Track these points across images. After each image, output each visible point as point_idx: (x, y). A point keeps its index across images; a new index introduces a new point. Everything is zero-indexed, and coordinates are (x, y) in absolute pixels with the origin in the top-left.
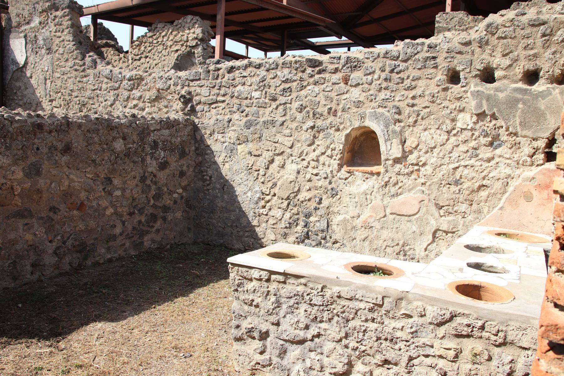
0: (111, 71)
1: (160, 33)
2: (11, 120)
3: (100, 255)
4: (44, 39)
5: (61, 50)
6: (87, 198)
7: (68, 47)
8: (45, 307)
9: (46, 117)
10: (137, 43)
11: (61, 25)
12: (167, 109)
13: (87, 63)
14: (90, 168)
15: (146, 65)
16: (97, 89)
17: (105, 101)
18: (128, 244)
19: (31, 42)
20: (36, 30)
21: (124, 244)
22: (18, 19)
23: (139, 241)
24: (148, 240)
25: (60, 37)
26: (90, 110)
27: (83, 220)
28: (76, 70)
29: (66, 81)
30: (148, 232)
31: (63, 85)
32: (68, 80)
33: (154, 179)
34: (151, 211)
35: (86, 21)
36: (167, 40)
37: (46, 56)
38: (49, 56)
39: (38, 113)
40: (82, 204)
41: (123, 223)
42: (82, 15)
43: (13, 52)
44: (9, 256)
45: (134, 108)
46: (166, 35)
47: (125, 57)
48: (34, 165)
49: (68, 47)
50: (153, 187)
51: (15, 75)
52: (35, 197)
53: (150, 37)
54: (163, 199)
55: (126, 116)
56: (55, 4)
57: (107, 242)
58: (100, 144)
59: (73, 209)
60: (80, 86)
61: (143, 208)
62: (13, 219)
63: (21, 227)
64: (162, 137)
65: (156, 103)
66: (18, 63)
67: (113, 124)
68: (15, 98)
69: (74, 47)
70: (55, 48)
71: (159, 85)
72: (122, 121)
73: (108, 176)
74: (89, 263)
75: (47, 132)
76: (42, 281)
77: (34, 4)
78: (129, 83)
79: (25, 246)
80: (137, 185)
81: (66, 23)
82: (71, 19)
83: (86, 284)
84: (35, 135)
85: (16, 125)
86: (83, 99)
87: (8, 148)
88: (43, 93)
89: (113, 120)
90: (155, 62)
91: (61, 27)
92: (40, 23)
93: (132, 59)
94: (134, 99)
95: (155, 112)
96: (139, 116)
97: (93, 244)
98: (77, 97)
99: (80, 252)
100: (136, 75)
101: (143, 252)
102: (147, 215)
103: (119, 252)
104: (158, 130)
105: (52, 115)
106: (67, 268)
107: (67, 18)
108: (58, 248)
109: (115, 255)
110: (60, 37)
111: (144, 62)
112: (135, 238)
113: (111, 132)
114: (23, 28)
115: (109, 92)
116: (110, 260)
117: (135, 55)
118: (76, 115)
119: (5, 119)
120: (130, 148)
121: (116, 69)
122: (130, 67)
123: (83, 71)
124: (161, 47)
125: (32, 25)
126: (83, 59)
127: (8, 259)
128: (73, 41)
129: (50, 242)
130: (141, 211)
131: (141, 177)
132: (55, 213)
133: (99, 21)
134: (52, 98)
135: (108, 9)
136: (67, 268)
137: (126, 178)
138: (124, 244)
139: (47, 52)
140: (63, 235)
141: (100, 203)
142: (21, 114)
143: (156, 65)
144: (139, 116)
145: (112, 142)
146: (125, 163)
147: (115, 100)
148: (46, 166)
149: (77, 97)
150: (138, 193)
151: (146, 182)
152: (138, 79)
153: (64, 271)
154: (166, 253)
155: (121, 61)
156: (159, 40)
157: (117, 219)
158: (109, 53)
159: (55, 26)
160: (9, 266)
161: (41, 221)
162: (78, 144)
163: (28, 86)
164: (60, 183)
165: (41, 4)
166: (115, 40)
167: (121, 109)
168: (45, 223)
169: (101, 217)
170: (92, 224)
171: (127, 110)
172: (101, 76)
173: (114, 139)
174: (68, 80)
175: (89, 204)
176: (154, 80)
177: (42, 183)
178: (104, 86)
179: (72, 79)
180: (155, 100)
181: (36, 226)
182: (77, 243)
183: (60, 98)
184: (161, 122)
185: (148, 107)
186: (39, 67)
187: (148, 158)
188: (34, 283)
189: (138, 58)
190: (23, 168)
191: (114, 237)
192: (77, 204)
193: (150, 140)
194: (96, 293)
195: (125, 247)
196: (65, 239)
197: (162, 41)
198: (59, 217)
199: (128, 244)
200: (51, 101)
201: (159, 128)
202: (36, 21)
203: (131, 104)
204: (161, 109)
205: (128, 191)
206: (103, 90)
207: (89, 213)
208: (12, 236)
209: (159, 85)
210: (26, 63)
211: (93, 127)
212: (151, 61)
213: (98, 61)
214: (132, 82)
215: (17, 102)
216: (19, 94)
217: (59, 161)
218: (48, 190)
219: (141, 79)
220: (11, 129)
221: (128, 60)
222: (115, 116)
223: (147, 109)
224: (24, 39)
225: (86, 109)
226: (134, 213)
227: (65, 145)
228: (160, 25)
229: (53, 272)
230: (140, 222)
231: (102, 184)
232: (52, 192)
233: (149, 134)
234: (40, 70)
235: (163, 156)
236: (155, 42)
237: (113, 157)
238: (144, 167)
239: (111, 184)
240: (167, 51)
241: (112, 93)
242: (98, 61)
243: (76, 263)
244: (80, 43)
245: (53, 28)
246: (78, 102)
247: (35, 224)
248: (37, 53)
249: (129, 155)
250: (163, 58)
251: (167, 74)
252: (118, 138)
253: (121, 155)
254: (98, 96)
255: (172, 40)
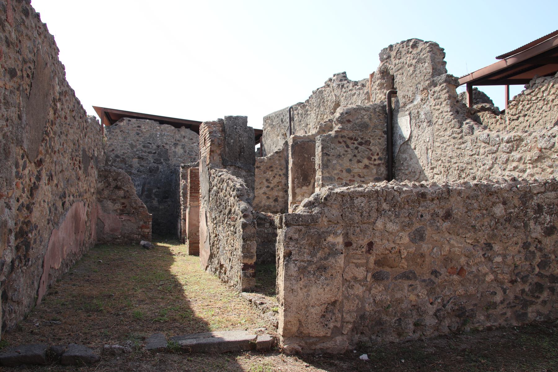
0: (488, 135)
1: (540, 89)
2: (400, 191)
3: (479, 322)
4: (425, 114)
5: (440, 122)
6: (467, 263)
7: (446, 117)
8: (425, 367)
9: (428, 186)
10: (513, 103)
11: (439, 98)
12: (552, 169)
13: (464, 130)
14: (469, 234)
15: (525, 124)
16: (474, 154)
17: (484, 165)
18: (509, 314)
19: (414, 117)
20: (419, 106)
21: (505, 314)
22: (404, 100)
23: (522, 311)
24: (532, 312)
25: (439, 109)
26: (469, 175)
27: (463, 285)
28: (454, 138)
29: (445, 149)
30: (532, 303)
31: (443, 153)
32: (447, 148)
33: (539, 246)
34: (536, 280)
35: (461, 89)
36: (548, 95)
37: (427, 128)
38: (430, 128)
39: (422, 183)
40: (462, 269)
41: (504, 291)
42: (457, 85)
43: (400, 129)
44: (395, 313)
45: (514, 170)
46: (546, 90)
47: (501, 119)
48: (418, 231)
49: (446, 117)
50: (538, 254)
51: (402, 148)
52: (418, 260)
53: (527, 95)
54: (550, 267)
55: (506, 181)
56: (433, 81)
57: (487, 309)
58: (479, 210)
59: (453, 273)
60: (459, 153)
61: (527, 276)
62: (400, 280)
63: (406, 288)
64: (546, 200)
65: (539, 164)
66: (404, 138)
67: (493, 189)
68: (402, 168)
69: (452, 117)
70: (434, 120)
71: (541, 144)
72: (502, 186)
73: (489, 241)
74: (468, 328)
75: (429, 200)
76: (422, 340)
77: (416, 85)
78: (508, 145)
79: (409, 305)
80: (519, 252)
81: (444, 95)
82: (448, 92)
83: (464, 350)
84: (419, 203)
85: (403, 195)
86: (461, 165)
87: (397, 216)
88: (425, 162)
89: (492, 185)
90: (535, 119)
91: (440, 100)
92: (422, 100)
93: (509, 120)
94: (513, 161)
95: (537, 173)
96: (520, 179)
97: (472, 310)
98: (456, 163)
99: (459, 316)
100: (515, 136)
101: (527, 324)
102: (531, 284)
103: (500, 321)
104: (542, 193)
105: (434, 184)
106: (446, 331)
107: (445, 91)
108: (438, 310)
109: (495, 324)
110: (439, 109)
111: (523, 121)
112: (517, 308)
113: (490, 197)
114: (408, 107)
115: (487, 156)
116: (490, 329)
117: (512, 115)
118: (456, 182)
119: (395, 190)
120: (511, 213)
121: (493, 132)
122: (507, 129)
123: (460, 138)
124: (541, 103)
125: (415, 103)
126: (460, 127)
127: (395, 316)
128: (450, 111)
129: (431, 304)
130: (524, 279)
131: (524, 243)
132: (436, 276)
133: (474, 87)
134: (433, 166)
135: (483, 75)
136: (446, 331)
137: (507, 244)
138: (505, 314)
139: (428, 124)
140: (443, 298)
141: (479, 269)
142: (408, 185)
143: (536, 122)
144: (520, 179)
145: (491, 207)
146: (505, 228)
147: (493, 164)
148: (428, 232)
149: (456, 163)
150: (520, 260)
151: (530, 249)
152: (517, 140)
153: (443, 334)
154: (555, 329)
155: (498, 123)
156: (538, 96)
157: (498, 286)
158: (486, 117)
159: (434, 100)
160: (395, 323)
161: (423, 284)
162: (458, 211)
163: (412, 156)
164: (441, 248)
165: (422, 83)
166: (490, 102)
167: (500, 172)
168: (427, 286)
169: (480, 283)
170: (472, 289)
171: (507, 173)
172: (478, 141)
173: (494, 204)
174: (447, 148)
175: (469, 269)
176: (535, 139)
177: (425, 247)
178: (482, 151)
179: (451, 147)
180: (536, 161)
181: (419, 288)
182: (457, 307)
183: (440, 165)
184: (545, 184)
185: (530, 168)
186: (422, 139)
187: (532, 223)
188: (416, 341)
189: (515, 117)
190: (409, 234)
191: (494, 305)
192: (457, 269)
193: (533, 203)
194: (474, 361)
195: (506, 316)
196: (445, 302)
197: (543, 96)
198: (440, 281)
199: (509, 314)
200: (432, 168)
201: (543, 191)
202: (419, 98)
203: (510, 166)
204: (545, 170)
205: (509, 258)
206: (480, 154)
207: (468, 279)
208: (398, 295)
209: (541, 144)
210: (411, 137)
211: (472, 193)
212: (531, 119)
213: (475, 127)
214: (510, 144)
215: (403, 171)
216: (405, 164)
217: (440, 227)
218: (430, 255)
219: (521, 140)
220: (399, 199)
221: (505, 121)
222: (494, 181)
223: (528, 171)
224: (408, 116)
225: (464, 174)
226: (516, 281)
227: (446, 212)
228: (539, 81)
229: (433, 333)
230: (523, 291)
231: (482, 249)
232: (434, 256)
233: (532, 197)
234: (423, 141)
235: (549, 220)
236: (534, 98)
237: (493, 222)
238: (527, 233)
239: (491, 250)
240: (549, 106)
241: (490, 156)
242: (475, 127)
243: (455, 327)
244: (457, 112)
245: (432, 102)
246: (457, 168)
247: (419, 286)
248: (419, 126)
249: (510, 220)
250: (545, 114)
251: (550, 132)
252: (498, 203)
253: (502, 220)
254: (476, 161)
255: (554, 94)
